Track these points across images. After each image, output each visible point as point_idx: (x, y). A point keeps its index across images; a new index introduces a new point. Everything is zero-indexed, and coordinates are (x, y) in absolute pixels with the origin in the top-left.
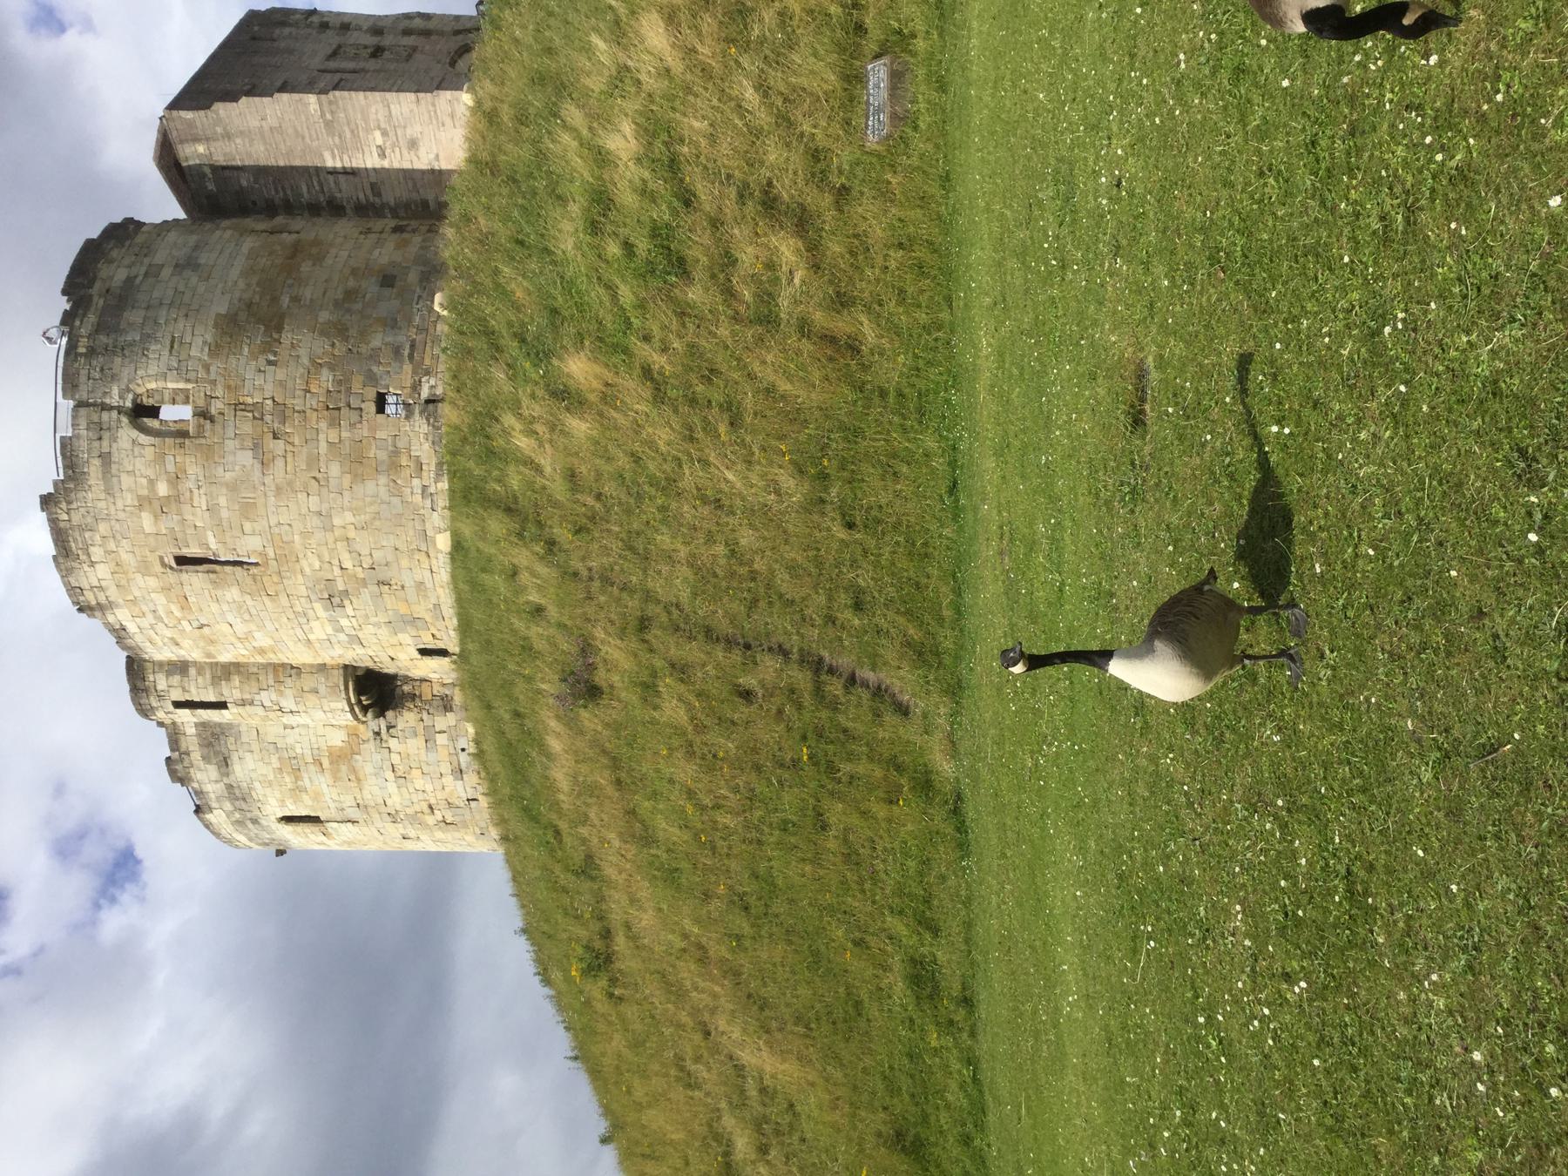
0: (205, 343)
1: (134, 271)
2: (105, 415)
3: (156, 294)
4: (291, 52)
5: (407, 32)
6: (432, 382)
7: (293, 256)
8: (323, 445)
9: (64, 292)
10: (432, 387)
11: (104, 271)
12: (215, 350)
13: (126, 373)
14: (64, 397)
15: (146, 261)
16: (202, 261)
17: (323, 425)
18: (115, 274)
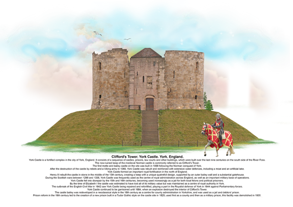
5: (157, 86)
11: (116, 53)
12: (106, 72)
13: (103, 61)
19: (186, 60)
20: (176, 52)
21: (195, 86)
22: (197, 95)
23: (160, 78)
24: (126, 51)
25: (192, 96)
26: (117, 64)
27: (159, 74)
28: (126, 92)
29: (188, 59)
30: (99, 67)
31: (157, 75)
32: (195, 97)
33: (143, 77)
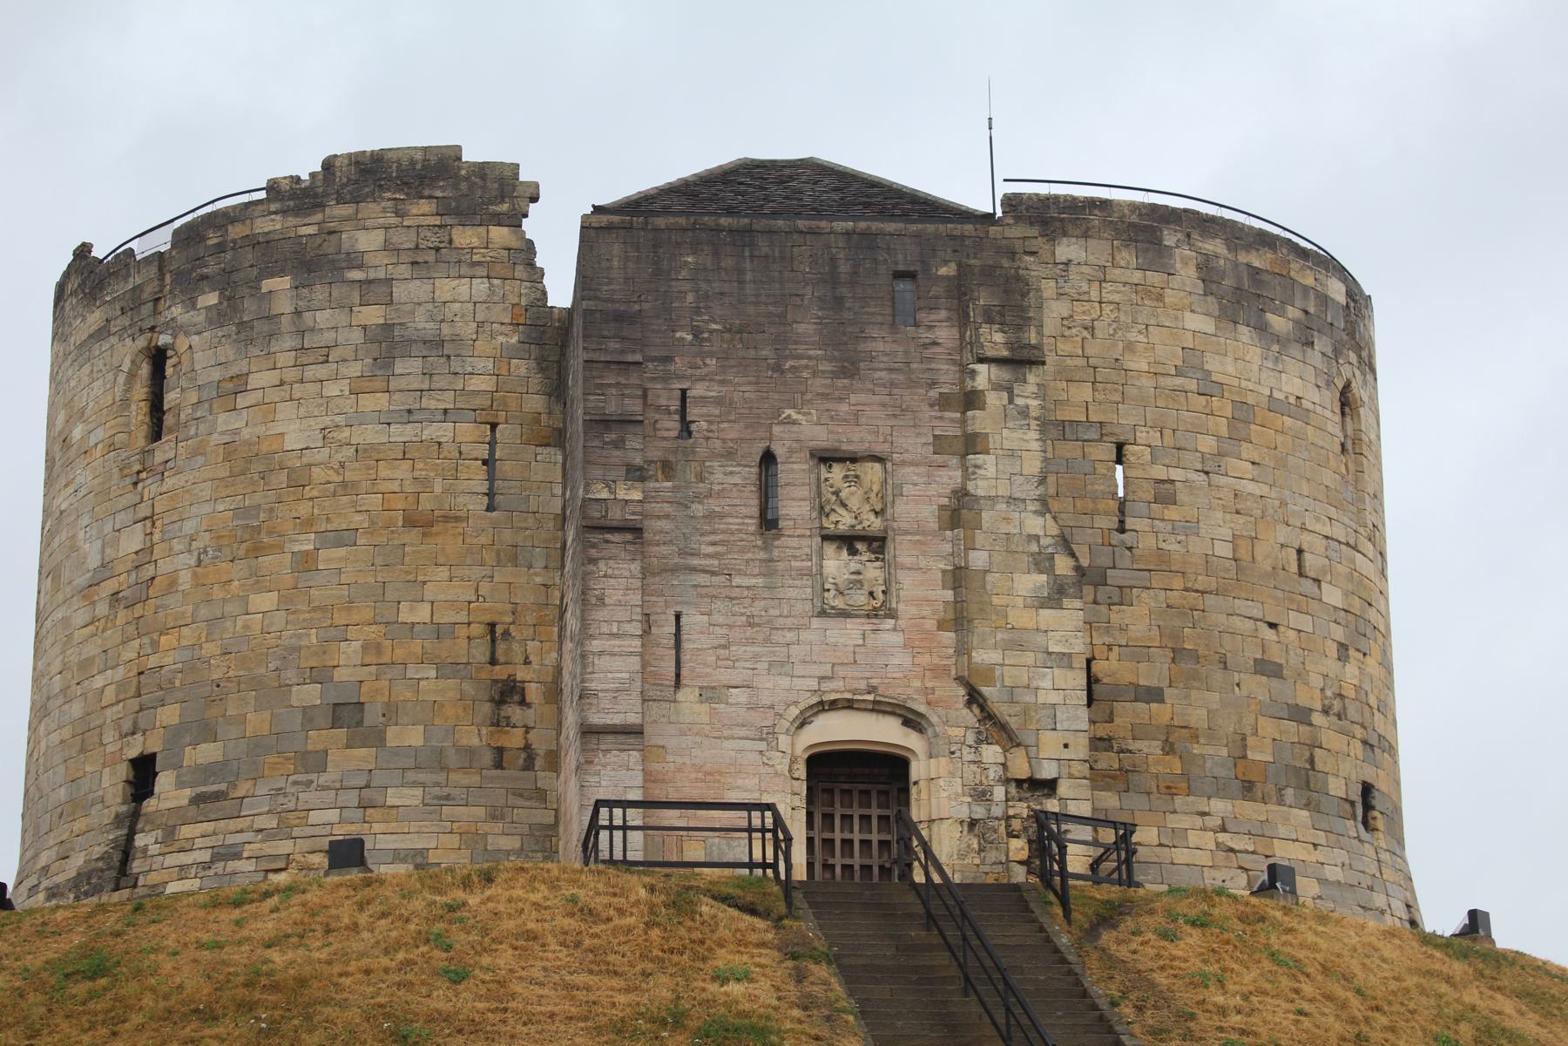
0: (236, 432)
1: (383, 259)
2: (147, 309)
3: (323, 318)
4: (849, 369)
5: (958, 577)
6: (154, 849)
7: (410, 523)
8: (98, 682)
9: (328, 164)
10: (145, 849)
14: (176, 233)
15: (404, 270)
16: (399, 367)
17: (120, 673)
18: (368, 235)
19: (1245, 332)
20: (1148, 229)
21: (1351, 671)
22: (1369, 774)
23: (989, 476)
24: (497, 195)
25: (1336, 787)
26: (387, 345)
27: (980, 421)
28: (508, 692)
29: (1262, 328)
30: (139, 413)
31: (940, 445)
32: (1356, 795)
33: (768, 458)
